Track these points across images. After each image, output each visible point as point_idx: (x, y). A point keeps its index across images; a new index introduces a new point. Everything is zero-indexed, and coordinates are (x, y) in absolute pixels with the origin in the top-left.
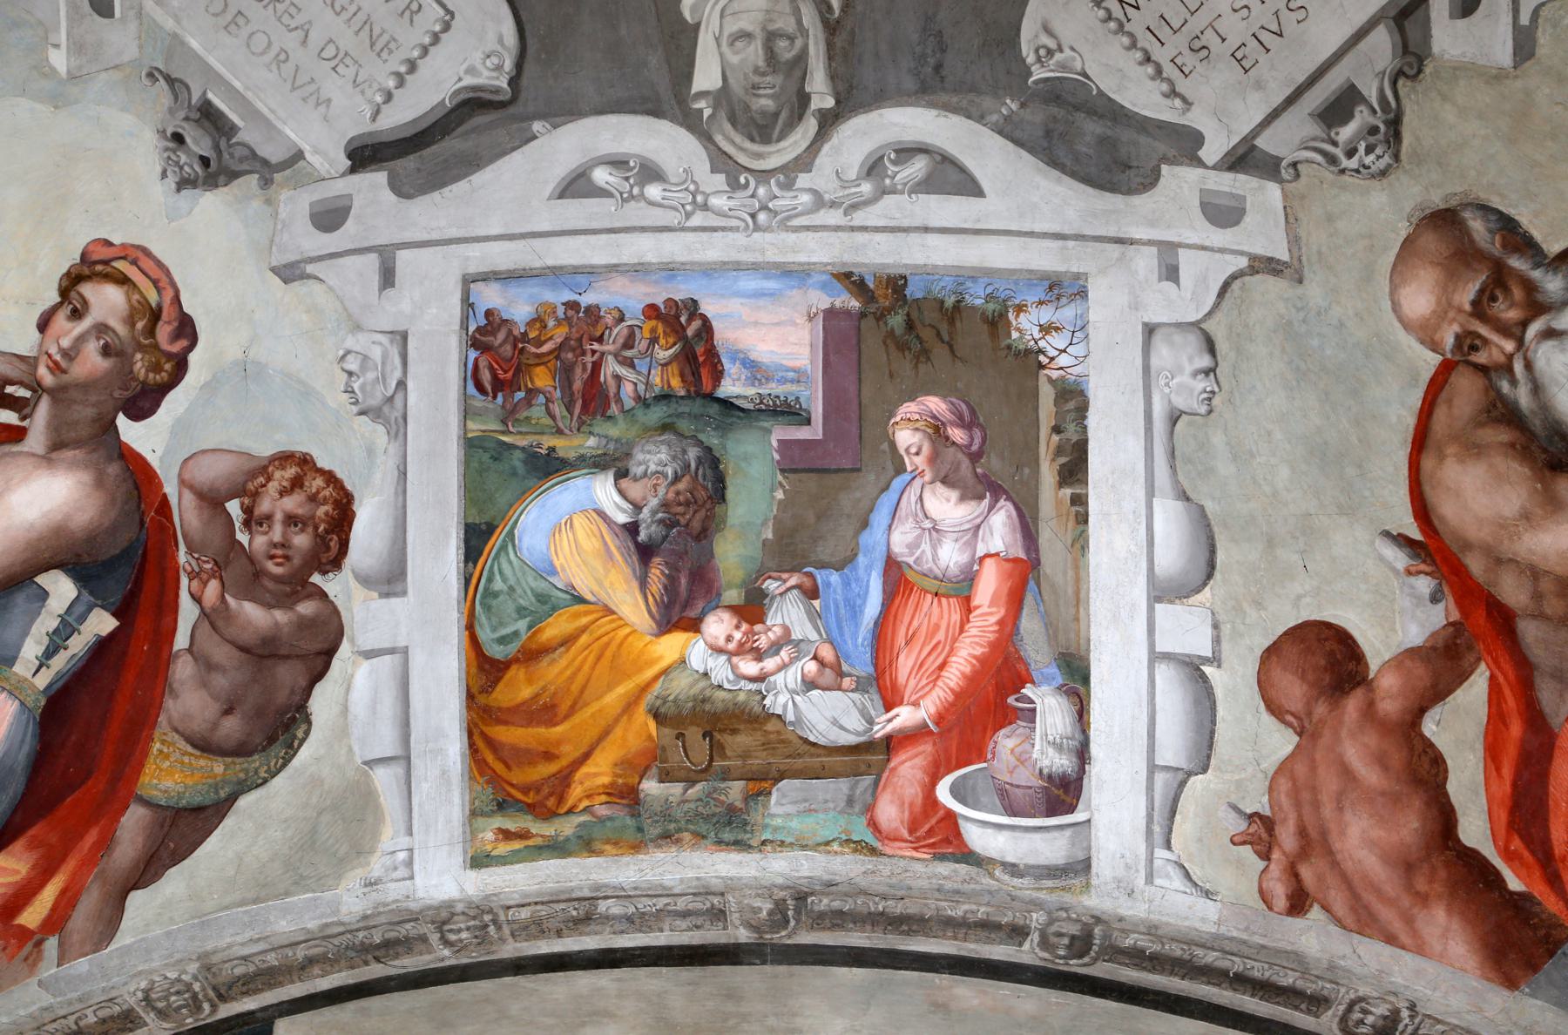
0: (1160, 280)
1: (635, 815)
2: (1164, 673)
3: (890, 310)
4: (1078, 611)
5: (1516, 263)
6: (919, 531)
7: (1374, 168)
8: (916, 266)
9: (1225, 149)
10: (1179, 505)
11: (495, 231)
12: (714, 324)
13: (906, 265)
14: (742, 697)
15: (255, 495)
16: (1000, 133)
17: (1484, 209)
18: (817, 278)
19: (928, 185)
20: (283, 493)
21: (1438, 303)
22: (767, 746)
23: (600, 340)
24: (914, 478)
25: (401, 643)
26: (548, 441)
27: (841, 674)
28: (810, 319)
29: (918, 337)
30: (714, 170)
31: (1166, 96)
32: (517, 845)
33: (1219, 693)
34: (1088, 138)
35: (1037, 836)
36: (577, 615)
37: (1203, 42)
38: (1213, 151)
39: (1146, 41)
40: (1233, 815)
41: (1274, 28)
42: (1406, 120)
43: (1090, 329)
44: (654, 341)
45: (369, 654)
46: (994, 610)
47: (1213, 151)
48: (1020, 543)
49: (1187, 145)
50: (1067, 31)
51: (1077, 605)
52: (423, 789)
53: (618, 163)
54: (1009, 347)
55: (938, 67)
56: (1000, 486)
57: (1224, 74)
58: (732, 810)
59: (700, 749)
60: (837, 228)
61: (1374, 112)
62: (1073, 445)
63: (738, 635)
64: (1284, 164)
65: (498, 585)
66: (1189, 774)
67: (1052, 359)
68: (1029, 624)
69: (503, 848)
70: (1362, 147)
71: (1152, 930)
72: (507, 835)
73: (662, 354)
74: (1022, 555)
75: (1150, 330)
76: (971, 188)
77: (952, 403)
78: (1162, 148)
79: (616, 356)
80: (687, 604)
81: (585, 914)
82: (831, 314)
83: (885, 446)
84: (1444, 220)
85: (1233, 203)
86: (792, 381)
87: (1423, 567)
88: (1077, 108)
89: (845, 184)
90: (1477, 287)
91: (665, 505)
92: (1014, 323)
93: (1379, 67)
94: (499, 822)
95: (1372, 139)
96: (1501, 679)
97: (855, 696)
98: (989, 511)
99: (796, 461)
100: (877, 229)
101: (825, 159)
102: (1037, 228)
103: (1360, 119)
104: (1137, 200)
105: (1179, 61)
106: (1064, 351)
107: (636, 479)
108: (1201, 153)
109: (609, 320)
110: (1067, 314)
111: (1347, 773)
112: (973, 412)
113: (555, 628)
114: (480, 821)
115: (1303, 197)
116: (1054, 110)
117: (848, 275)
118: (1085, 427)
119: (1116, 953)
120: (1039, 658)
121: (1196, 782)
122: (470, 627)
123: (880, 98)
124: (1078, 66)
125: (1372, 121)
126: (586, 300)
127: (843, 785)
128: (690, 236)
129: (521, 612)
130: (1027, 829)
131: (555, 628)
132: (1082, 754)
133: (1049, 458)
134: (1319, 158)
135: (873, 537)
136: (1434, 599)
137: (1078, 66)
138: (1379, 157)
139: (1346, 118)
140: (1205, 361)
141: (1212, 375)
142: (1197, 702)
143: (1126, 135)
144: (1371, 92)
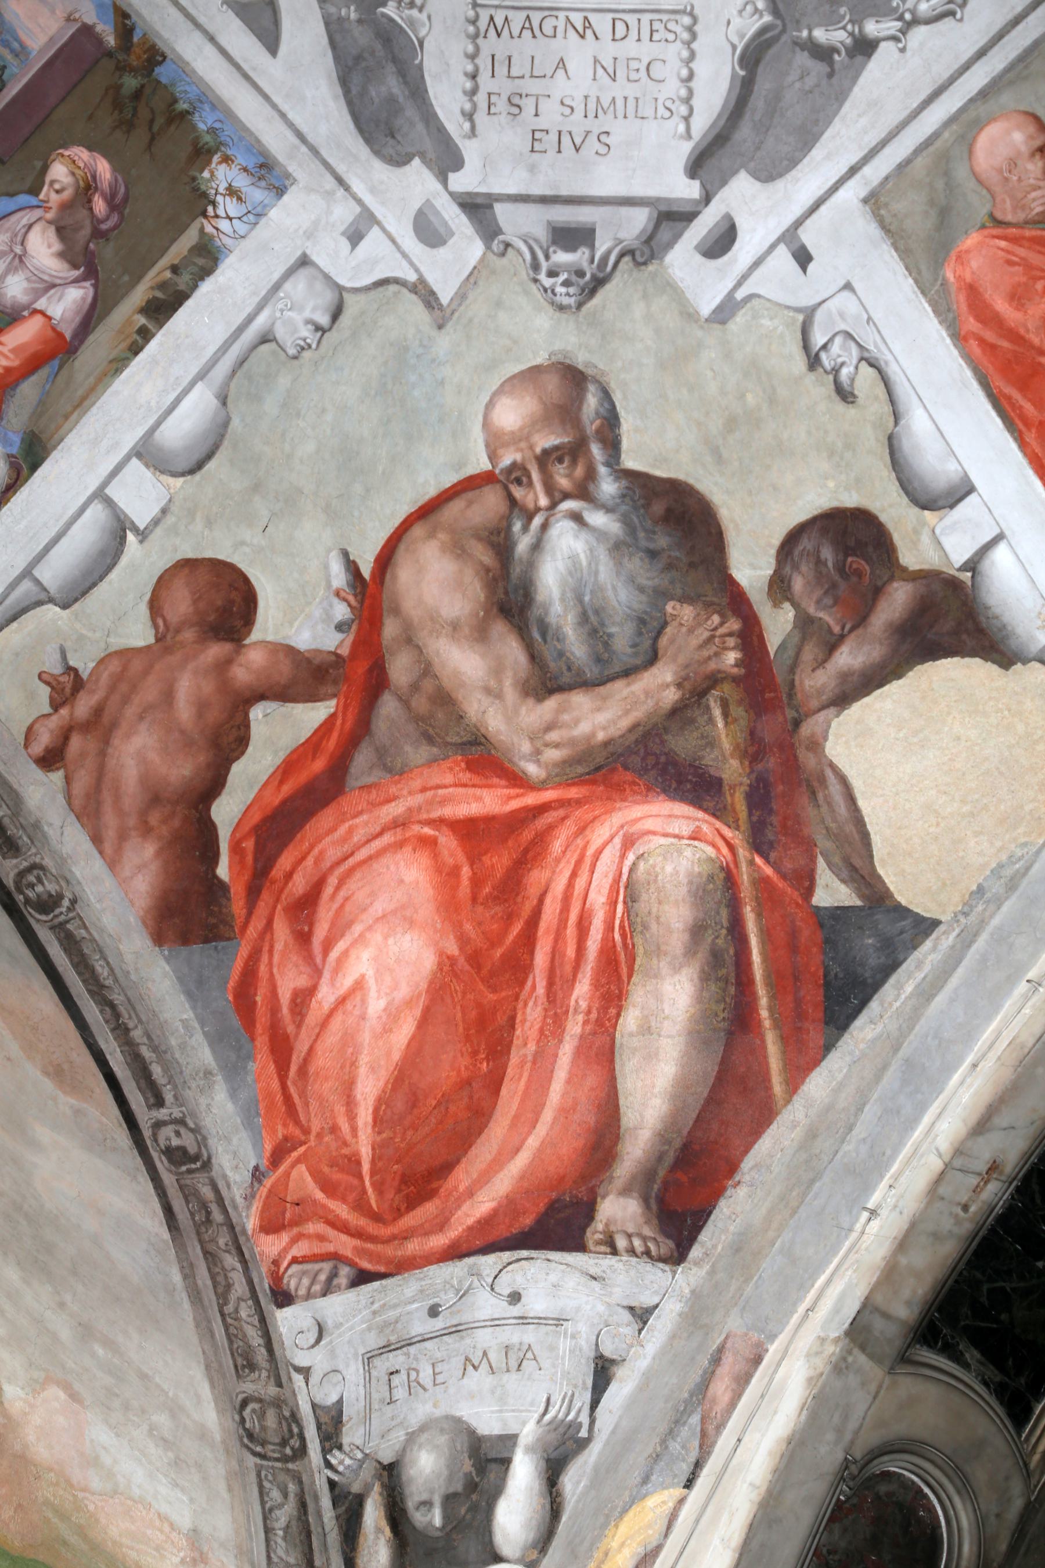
0: (343, 234)
2: (97, 512)
3: (132, 70)
4: (72, 413)
5: (596, 451)
6: (5, 248)
7: (558, 299)
8: (180, 58)
9: (470, 189)
10: (215, 402)
13: (174, 50)
16: (327, 24)
17: (606, 395)
21: (521, 429)
24: (38, 207)
28: (69, 19)
29: (135, 109)
31: (463, 113)
33: (124, 561)
34: (383, 89)
37: (522, 103)
38: (460, 182)
39: (484, 62)
40: (57, 656)
41: (578, 141)
43: (263, 221)
46: (11, 356)
47: (460, 182)
48: (74, 325)
51: (76, 407)
54: (194, 179)
56: (97, 271)
57: (516, 139)
61: (592, 261)
62: (176, 291)
64: (501, 237)
66: (51, 600)
67: (217, 216)
68: (29, 390)
70: (563, 277)
74: (68, 336)
75: (304, 261)
76: (271, 42)
77: (116, 180)
78: (428, 145)
82: (86, 31)
83: (38, 164)
85: (442, 230)
86: (12, 51)
87: (351, 598)
88: (395, 60)
90: (557, 441)
92: (213, 165)
93: (621, 235)
95: (574, 278)
96: (339, 722)
98: (73, 282)
102: (291, 115)
104: (378, 165)
105: (493, 99)
106: (231, 219)
108: (452, 177)
110: (256, 195)
111: (168, 696)
112: (126, 199)
115: (493, 272)
116: (378, 47)
117: (126, 16)
118: (195, 287)
120: (14, 421)
121: (51, 611)
124: (423, 32)
125: (585, 265)
133: (149, 285)
134: (528, 256)
136: (340, 627)
137: (423, 32)
138: (568, 294)
140: (324, 320)
141: (319, 334)
142: (102, 553)
143: (411, 112)
144: (602, 246)
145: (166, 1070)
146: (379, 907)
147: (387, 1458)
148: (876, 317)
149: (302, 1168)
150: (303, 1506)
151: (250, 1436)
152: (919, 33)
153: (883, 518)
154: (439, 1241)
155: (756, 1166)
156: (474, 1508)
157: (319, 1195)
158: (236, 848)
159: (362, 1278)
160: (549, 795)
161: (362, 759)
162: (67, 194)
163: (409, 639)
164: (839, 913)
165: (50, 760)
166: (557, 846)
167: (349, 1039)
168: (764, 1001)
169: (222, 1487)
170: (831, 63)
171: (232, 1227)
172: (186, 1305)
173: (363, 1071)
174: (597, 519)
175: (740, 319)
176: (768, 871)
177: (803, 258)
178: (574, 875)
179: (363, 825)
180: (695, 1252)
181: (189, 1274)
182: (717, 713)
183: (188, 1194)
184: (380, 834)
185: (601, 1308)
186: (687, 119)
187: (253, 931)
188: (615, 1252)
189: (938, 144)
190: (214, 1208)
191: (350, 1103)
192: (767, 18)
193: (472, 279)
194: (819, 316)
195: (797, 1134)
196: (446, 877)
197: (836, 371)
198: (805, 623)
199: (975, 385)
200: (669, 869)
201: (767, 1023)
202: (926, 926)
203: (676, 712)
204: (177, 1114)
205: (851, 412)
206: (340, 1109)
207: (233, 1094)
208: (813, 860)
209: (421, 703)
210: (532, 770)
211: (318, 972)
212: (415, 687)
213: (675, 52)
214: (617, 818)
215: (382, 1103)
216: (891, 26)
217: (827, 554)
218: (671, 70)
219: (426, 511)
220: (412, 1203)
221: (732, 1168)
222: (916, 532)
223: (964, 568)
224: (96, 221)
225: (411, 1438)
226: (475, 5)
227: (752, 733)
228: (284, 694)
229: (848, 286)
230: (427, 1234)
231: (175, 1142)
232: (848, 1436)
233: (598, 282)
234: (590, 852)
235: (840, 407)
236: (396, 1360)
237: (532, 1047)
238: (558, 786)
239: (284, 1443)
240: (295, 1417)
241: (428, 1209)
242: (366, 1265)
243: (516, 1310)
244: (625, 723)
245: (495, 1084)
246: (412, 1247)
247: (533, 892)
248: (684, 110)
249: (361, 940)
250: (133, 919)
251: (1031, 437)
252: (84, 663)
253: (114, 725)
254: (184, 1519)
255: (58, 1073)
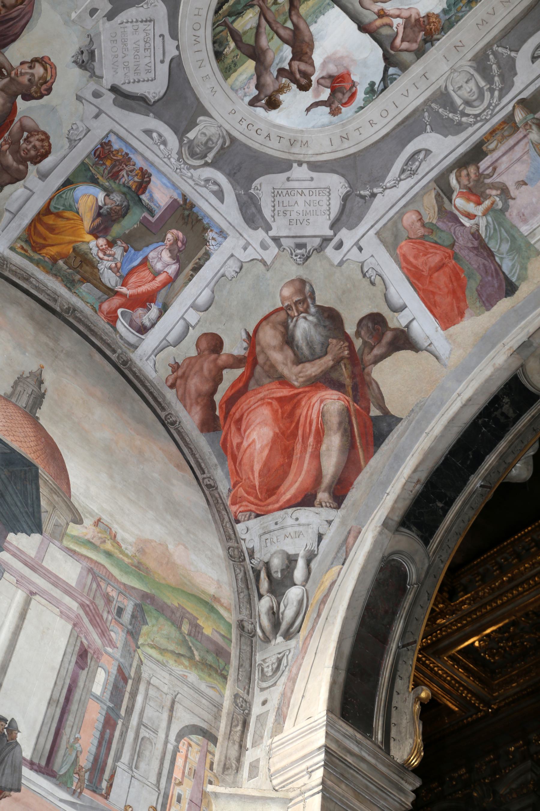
1: (53, 266)
2: (182, 322)
3: (187, 209)
5: (309, 300)
10: (211, 293)
11: (125, 126)
12: (151, 183)
14: (94, 260)
15: (32, 136)
17: (311, 286)
18: (178, 191)
19: (214, 193)
20: (38, 140)
22: (91, 273)
23: (126, 166)
25: (34, 191)
26: (99, 176)
27: (118, 271)
30: (177, 153)
32: (23, 252)
33: (189, 334)
35: (131, 334)
36: (75, 216)
38: (271, 233)
39: (277, 203)
42: (311, 258)
44: (137, 175)
45: (26, 187)
47: (271, 233)
49: (268, 228)
50: (264, 188)
52: (13, 224)
53: (160, 136)
55: (235, 173)
57: (286, 222)
58: (74, 280)
59: (78, 263)
60: (190, 185)
63: (104, 247)
65: (64, 196)
66: (171, 345)
68: (163, 292)
69: (19, 250)
71: (140, 370)
72: (22, 248)
73: (136, 179)
75: (232, 255)
76: (222, 201)
78: (263, 224)
79: (127, 171)
80: (99, 232)
81: (27, 278)
82: (175, 200)
84: (303, 282)
88: (254, 203)
89: (199, 178)
91: (111, 209)
94: (23, 244)
97: (118, 278)
99: (144, 223)
100: (198, 192)
101: (199, 171)
103: (302, 251)
107: (110, 199)
108: (269, 232)
109: (132, 163)
110: (219, 239)
111: (202, 369)
113: (68, 214)
114: (19, 241)
116: (249, 200)
117: (185, 196)
119: (130, 370)
121: (171, 348)
122: (51, 199)
123: (219, 169)
126: (131, 156)
127: (100, 294)
128: (161, 162)
129: (64, 205)
130: (130, 331)
131: (68, 214)
132: (153, 325)
135: (147, 250)
136: (245, 349)
139: (301, 249)
140: (238, 270)
142: (183, 333)
143: (258, 216)
144: (308, 248)
145: (205, 464)
146: (258, 421)
147: (266, 561)
148: (380, 263)
149: (241, 488)
150: (245, 573)
151: (231, 556)
152: (387, 191)
153: (384, 315)
154: (277, 506)
155: (358, 483)
156: (289, 572)
157: (246, 495)
158: (220, 407)
159: (258, 516)
160: (301, 390)
161: (252, 382)
162: (171, 242)
163: (263, 351)
164: (377, 417)
165: (172, 386)
166: (303, 403)
167: (252, 455)
168: (358, 441)
169: (225, 570)
170: (365, 199)
171: (224, 504)
172: (213, 524)
173: (255, 463)
174: (310, 318)
175: (345, 265)
176: (358, 407)
177: (360, 249)
178: (308, 410)
179: (253, 400)
180: (343, 506)
181: (213, 517)
182: (343, 367)
183: (212, 496)
184: (257, 402)
185: (319, 521)
186: (329, 215)
187: (226, 428)
188: (322, 507)
189: (394, 219)
190: (219, 499)
191: (253, 471)
192: (348, 189)
193: (276, 258)
194: (365, 264)
195: (368, 475)
196: (275, 412)
197: (370, 278)
198: (365, 343)
199: (406, 280)
200: (332, 408)
201: (359, 447)
202: (399, 420)
203: (333, 367)
204: (208, 476)
205: (374, 288)
206: (250, 473)
207: (222, 470)
208: (369, 404)
209: (266, 368)
210: (296, 384)
211: (243, 438)
212: (265, 364)
213: (325, 198)
214: (318, 395)
215: (261, 471)
216: (380, 190)
217: (370, 325)
218: (324, 202)
219: (266, 318)
220: (270, 496)
221: (352, 484)
222: (393, 318)
223: (405, 327)
224: (179, 248)
225: (272, 556)
226: (274, 189)
227: (352, 372)
228: (231, 367)
229: (372, 256)
230: (274, 504)
231: (208, 483)
232: (383, 550)
233: (308, 257)
234: (312, 404)
235: (372, 287)
236: (267, 536)
237: (299, 455)
238: (303, 388)
239: (240, 558)
240: (242, 551)
241: (274, 498)
242: (259, 512)
243: (297, 522)
244: (319, 371)
245: (290, 465)
246: (270, 507)
247: (297, 415)
248: (328, 213)
249: (253, 429)
250: (195, 426)
251: (421, 293)
252: (180, 361)
253: (188, 377)
254: (215, 577)
255: (178, 466)
